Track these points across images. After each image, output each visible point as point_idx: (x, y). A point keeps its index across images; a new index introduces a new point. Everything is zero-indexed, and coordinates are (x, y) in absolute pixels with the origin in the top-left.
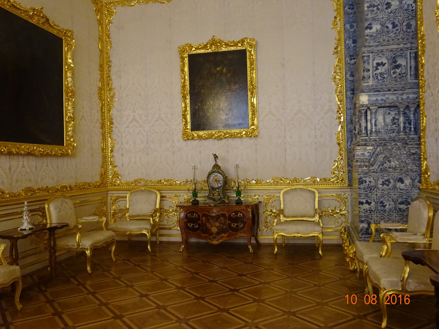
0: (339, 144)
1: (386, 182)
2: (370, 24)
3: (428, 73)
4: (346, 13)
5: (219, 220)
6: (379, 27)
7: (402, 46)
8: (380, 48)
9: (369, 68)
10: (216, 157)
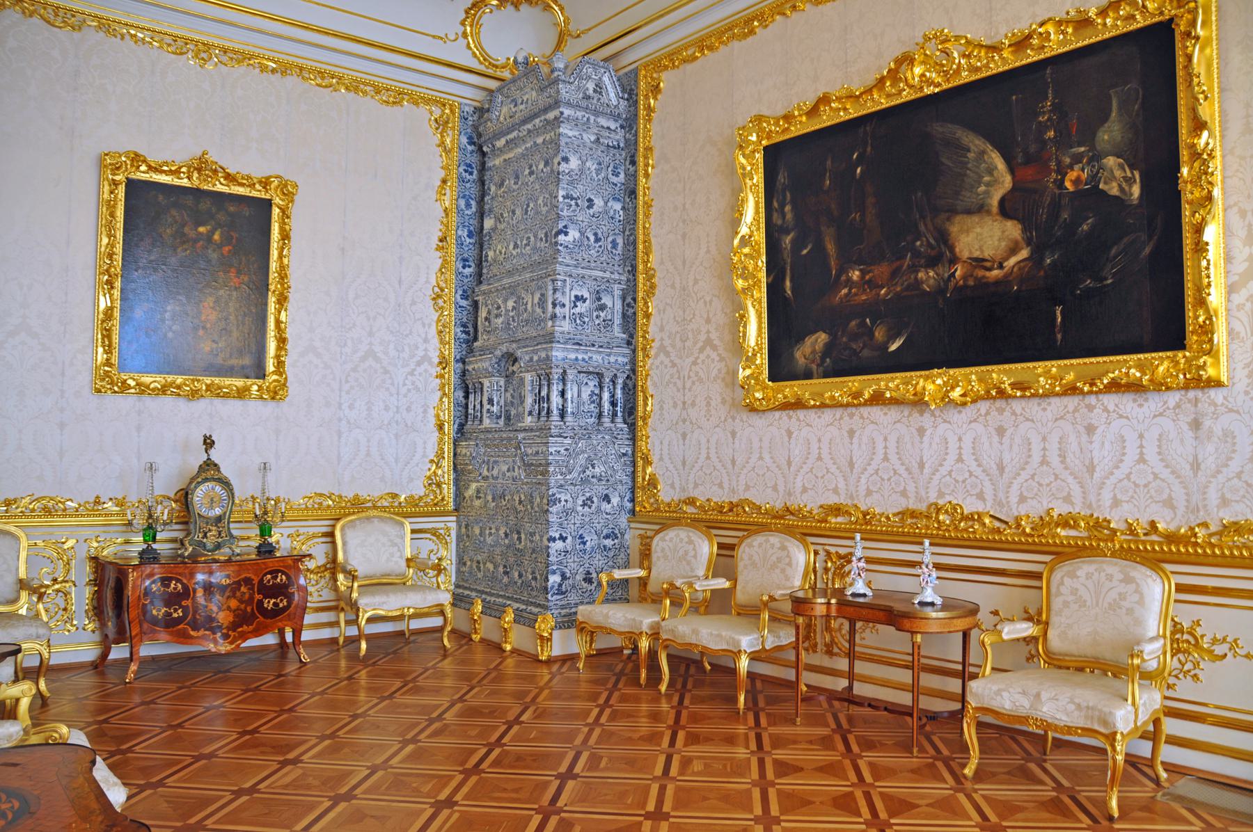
0: (441, 427)
1: (587, 502)
2: (565, 227)
3: (662, 329)
4: (462, 180)
5: (238, 594)
6: (577, 235)
7: (607, 275)
8: (581, 271)
9: (563, 301)
10: (209, 443)
